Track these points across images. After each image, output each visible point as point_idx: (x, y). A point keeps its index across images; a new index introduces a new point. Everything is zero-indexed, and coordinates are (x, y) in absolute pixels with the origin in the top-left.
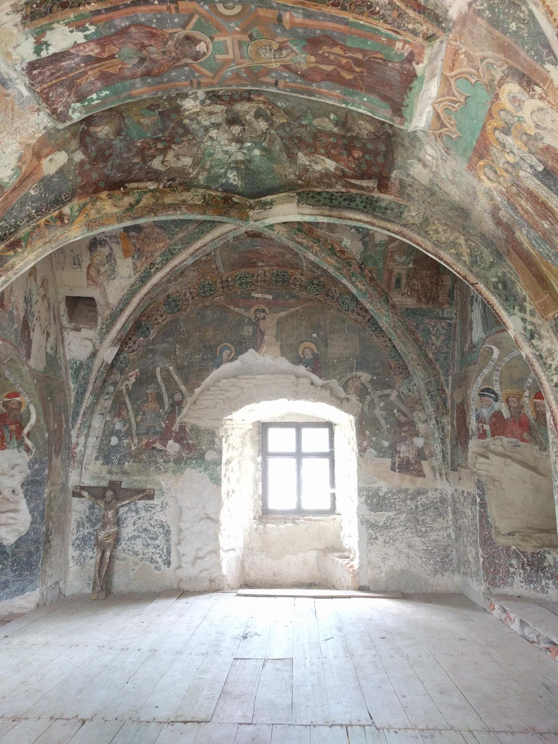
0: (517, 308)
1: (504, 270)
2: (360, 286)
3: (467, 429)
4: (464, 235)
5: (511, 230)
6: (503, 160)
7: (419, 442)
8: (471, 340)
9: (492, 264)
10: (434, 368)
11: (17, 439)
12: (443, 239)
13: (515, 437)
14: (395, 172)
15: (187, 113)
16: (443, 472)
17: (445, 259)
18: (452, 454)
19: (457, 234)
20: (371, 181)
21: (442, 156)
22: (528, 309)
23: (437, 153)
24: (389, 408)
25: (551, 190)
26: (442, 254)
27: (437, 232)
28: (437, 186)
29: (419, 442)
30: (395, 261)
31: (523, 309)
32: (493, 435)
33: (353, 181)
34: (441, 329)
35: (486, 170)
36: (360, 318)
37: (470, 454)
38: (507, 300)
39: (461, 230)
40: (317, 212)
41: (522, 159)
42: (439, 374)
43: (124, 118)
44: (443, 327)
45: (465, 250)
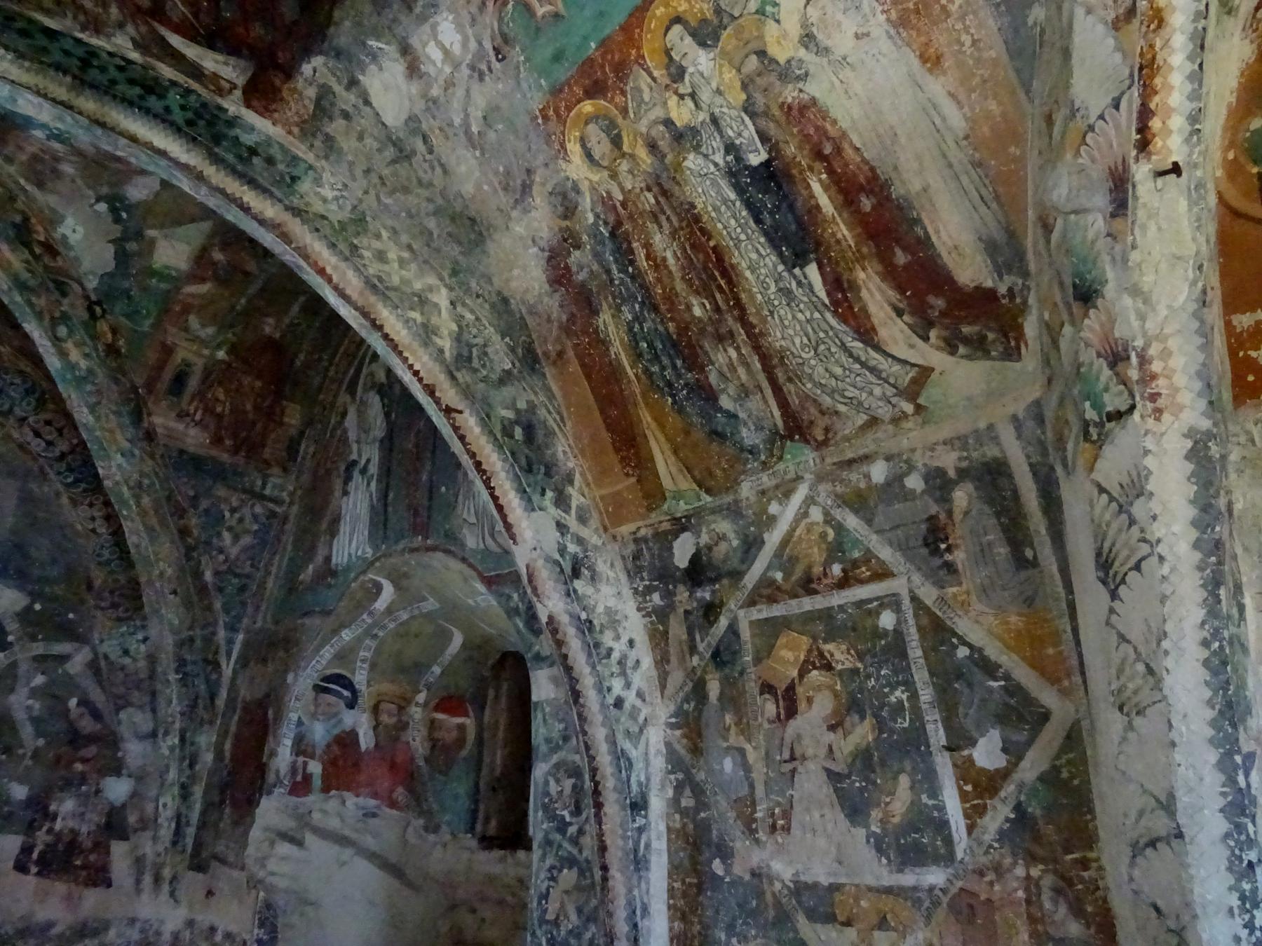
0: (550, 494)
1: (533, 397)
2: (75, 355)
3: (262, 769)
4: (451, 289)
5: (590, 304)
6: (658, 113)
7: (117, 789)
8: (328, 559)
9: (505, 378)
10: (209, 608)
12: (396, 280)
13: (375, 795)
14: (318, 61)
16: (167, 873)
17: (387, 330)
18: (202, 825)
19: (432, 280)
20: (232, 60)
21: (480, 54)
22: (574, 504)
23: (465, 44)
24: (53, 695)
25: (758, 221)
26: (385, 314)
27: (381, 256)
28: (425, 139)
29: (117, 789)
30: (186, 330)
31: (562, 501)
32: (326, 789)
33: (175, 40)
34: (248, 518)
35: (592, 129)
36: (37, 445)
37: (255, 833)
38: (529, 470)
39: (445, 274)
40: (26, 78)
41: (715, 121)
42: (215, 623)
44: (255, 517)
45: (446, 324)
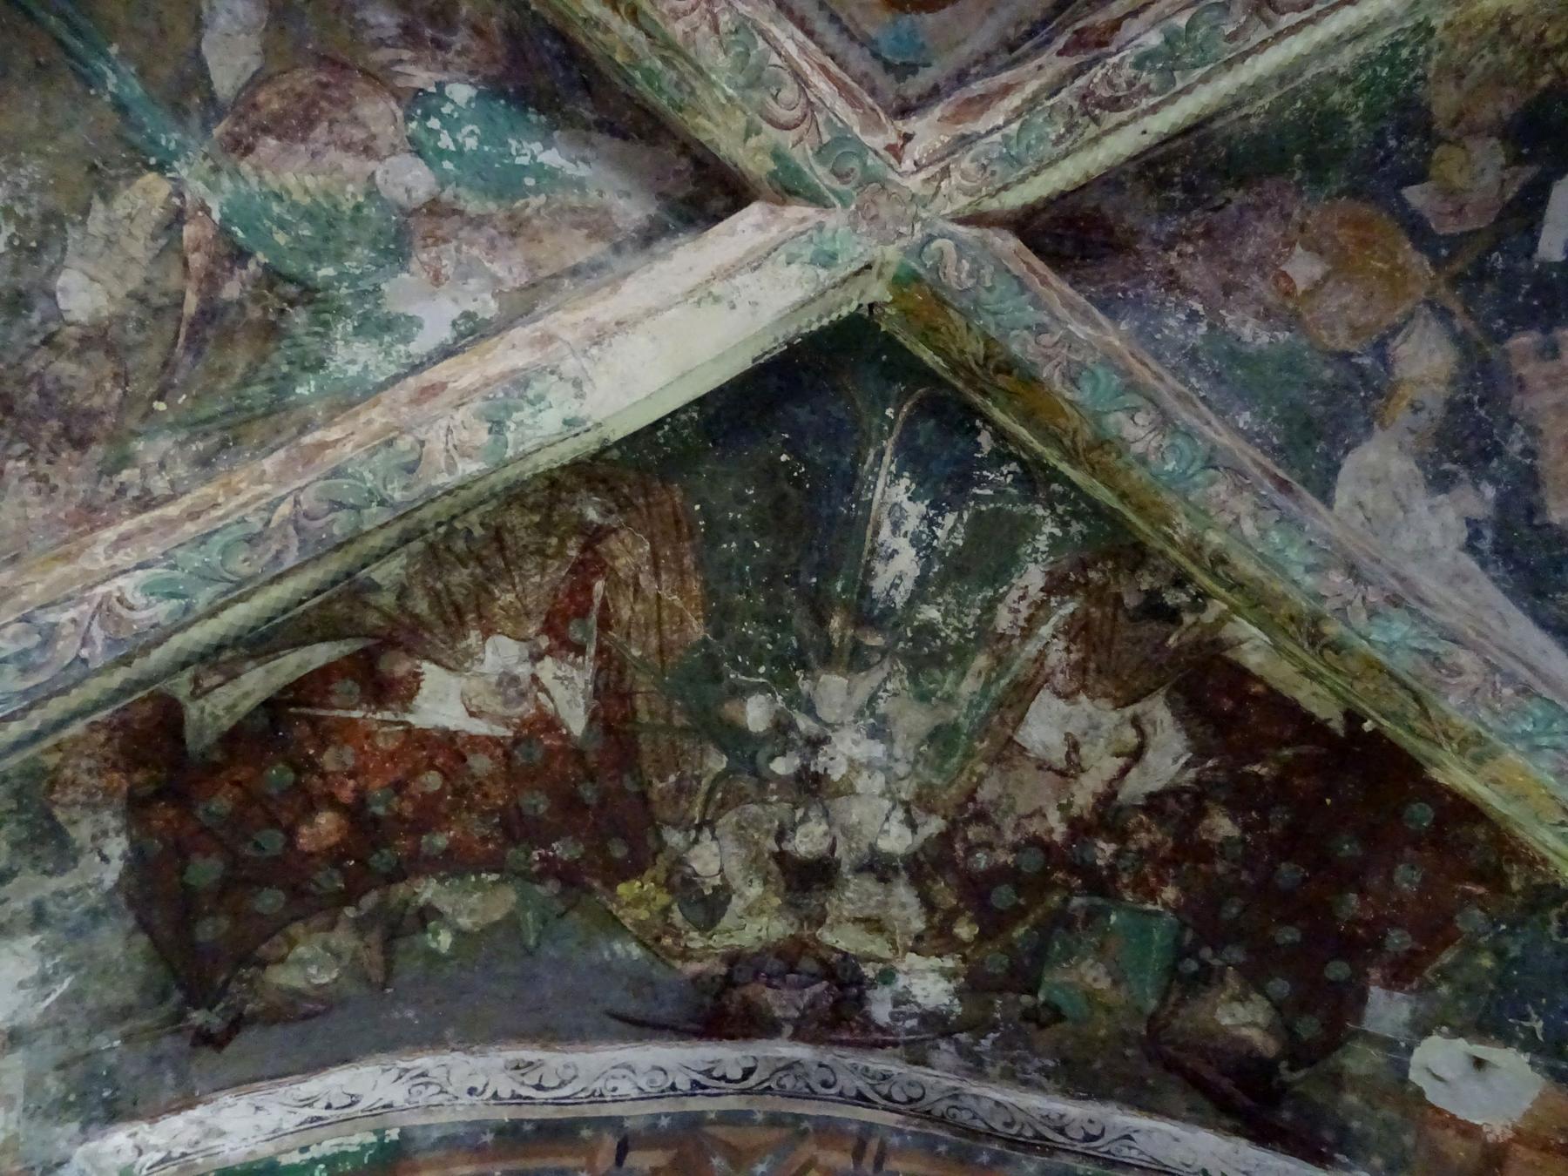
14: (111, 875)
15: (949, 963)
20: (227, 723)
33: (321, 654)
43: (1153, 1018)
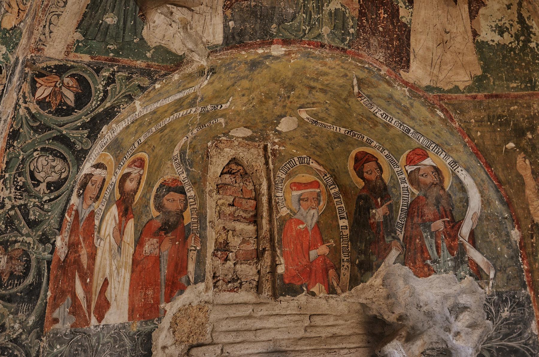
11: (450, 249)
